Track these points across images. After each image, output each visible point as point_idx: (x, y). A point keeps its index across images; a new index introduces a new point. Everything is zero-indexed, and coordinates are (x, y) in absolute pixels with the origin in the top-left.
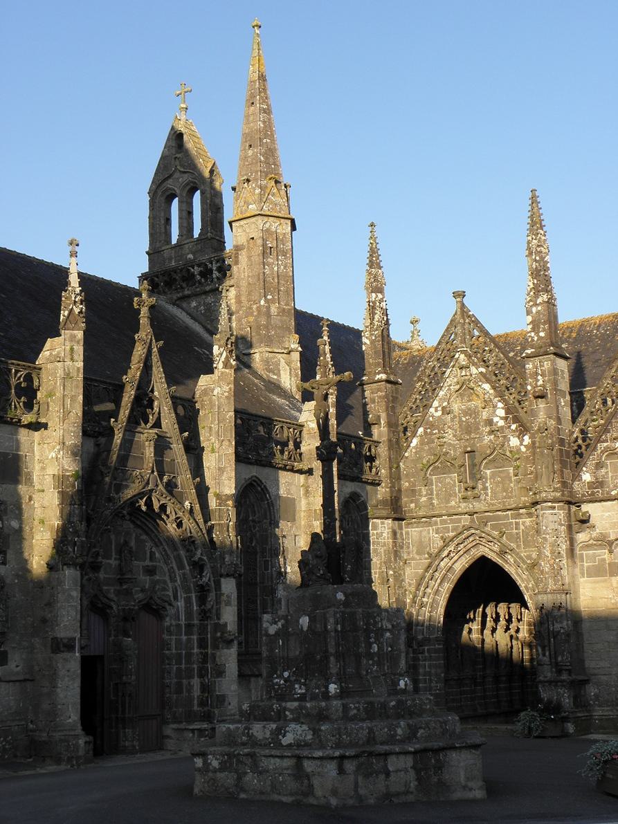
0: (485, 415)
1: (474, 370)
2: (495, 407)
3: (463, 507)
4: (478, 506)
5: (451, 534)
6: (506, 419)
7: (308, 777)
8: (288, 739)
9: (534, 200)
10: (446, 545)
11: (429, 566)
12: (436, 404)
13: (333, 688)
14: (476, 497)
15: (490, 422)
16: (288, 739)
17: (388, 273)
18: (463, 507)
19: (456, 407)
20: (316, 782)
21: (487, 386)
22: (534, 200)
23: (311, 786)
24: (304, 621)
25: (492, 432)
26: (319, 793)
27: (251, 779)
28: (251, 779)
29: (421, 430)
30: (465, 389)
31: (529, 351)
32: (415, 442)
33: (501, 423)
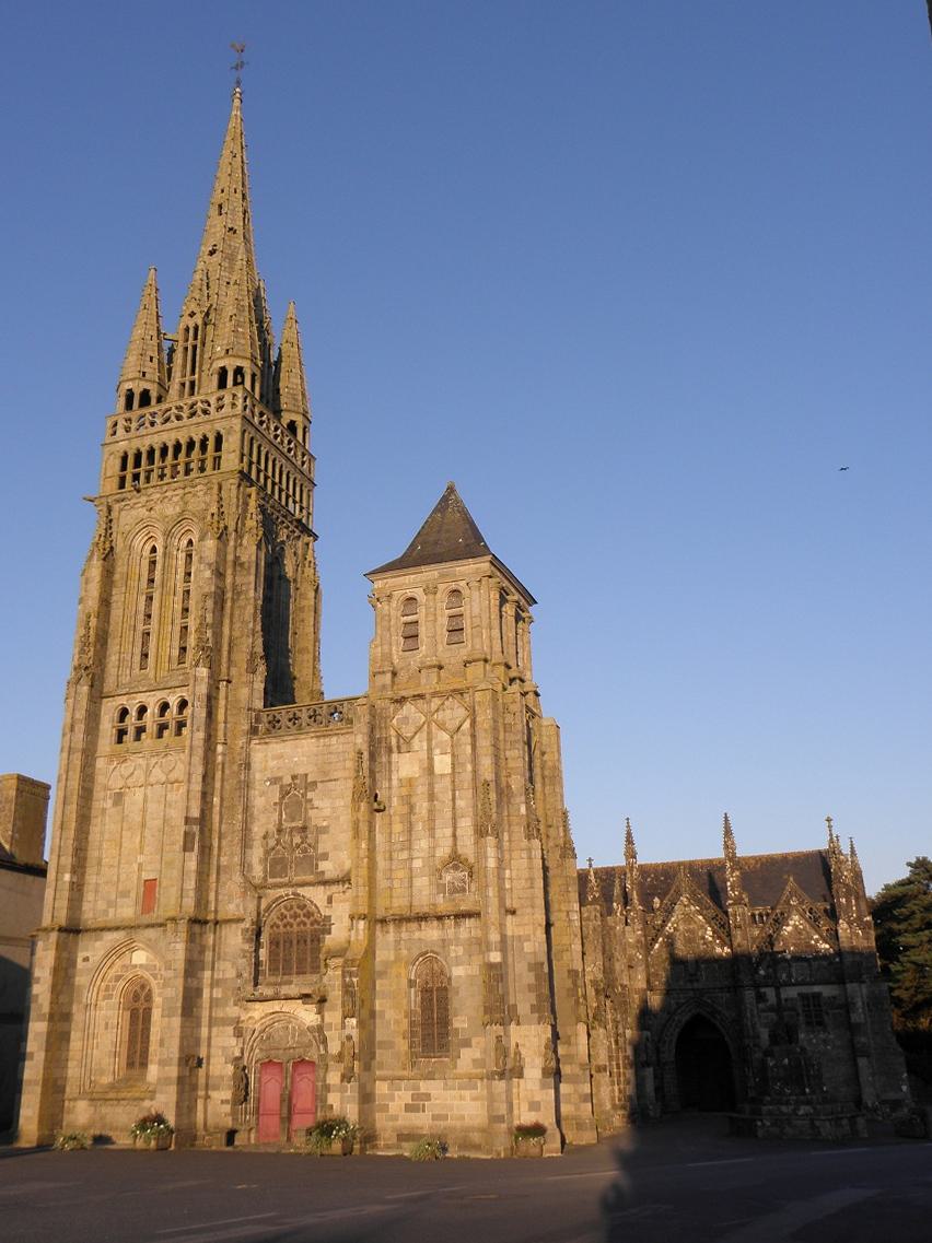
0: (700, 934)
1: (692, 908)
2: (706, 930)
3: (689, 986)
4: (696, 985)
5: (683, 1001)
6: (713, 937)
7: (818, 1128)
8: (801, 1112)
9: (726, 818)
10: (679, 1008)
11: (669, 1020)
12: (670, 925)
13: (807, 1090)
14: (697, 981)
15: (703, 938)
16: (801, 1112)
17: (637, 847)
18: (689, 986)
19: (681, 928)
20: (822, 1130)
21: (701, 917)
22: (726, 818)
23: (819, 1132)
24: (786, 1061)
25: (704, 944)
26: (824, 1134)
27: (788, 1130)
28: (788, 1130)
29: (661, 939)
30: (688, 919)
31: (730, 902)
32: (657, 946)
33: (710, 939)
